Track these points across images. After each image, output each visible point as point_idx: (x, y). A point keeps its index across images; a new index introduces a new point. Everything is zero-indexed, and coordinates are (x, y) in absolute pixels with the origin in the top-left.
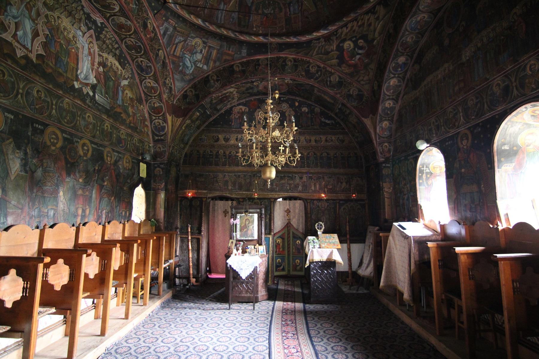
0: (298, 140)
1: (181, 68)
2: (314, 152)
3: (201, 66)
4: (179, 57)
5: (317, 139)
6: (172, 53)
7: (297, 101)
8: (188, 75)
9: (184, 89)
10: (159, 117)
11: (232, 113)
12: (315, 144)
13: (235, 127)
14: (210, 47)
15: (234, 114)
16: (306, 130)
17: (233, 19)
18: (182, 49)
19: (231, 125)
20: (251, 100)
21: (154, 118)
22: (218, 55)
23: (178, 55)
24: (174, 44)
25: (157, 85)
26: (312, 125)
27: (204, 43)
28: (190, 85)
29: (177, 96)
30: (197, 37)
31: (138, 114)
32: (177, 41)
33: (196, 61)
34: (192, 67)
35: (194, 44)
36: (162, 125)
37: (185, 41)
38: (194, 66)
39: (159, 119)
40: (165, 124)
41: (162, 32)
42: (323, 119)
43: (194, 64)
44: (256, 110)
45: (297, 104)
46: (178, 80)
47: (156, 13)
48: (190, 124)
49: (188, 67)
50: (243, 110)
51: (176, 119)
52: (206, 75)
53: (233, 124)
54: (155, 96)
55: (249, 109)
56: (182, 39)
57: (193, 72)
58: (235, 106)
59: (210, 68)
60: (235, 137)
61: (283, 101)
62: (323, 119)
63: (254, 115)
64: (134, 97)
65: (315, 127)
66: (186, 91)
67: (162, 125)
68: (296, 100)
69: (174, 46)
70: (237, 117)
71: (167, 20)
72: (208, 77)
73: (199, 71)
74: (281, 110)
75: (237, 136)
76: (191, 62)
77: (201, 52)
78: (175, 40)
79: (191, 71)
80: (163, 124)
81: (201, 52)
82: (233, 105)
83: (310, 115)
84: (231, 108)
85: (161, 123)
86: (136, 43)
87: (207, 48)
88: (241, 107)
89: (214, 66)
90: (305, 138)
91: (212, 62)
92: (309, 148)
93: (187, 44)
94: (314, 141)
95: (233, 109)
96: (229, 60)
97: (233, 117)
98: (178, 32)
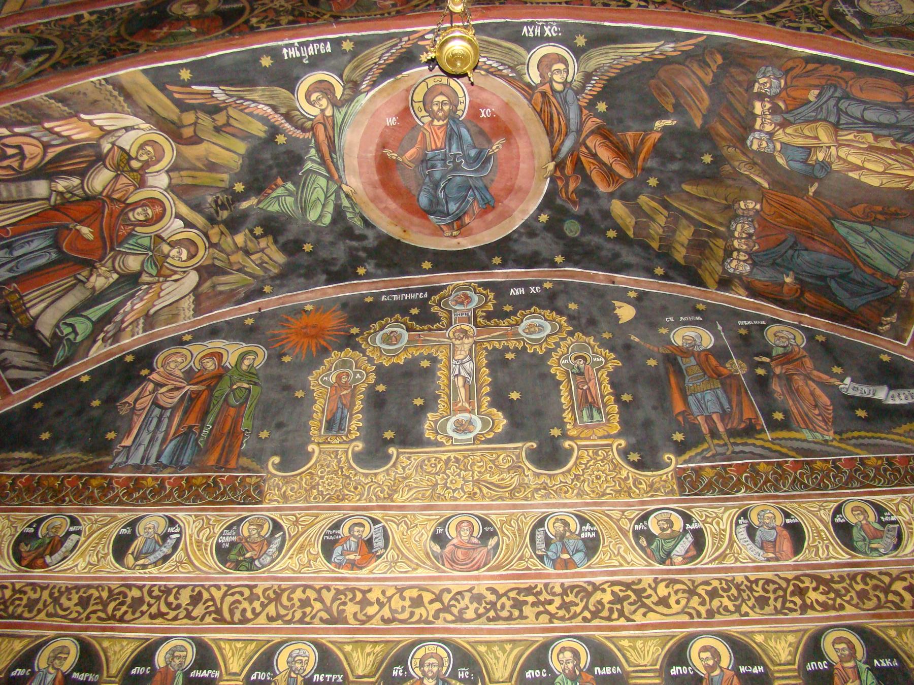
0: (677, 537)
2: (861, 632)
5: (849, 516)
7: (629, 301)
11: (145, 378)
12: (844, 556)
13: (136, 460)
15: (159, 385)
16: (736, 455)
19: (106, 447)
20: (299, 311)
26: (774, 426)
42: (848, 386)
44: (324, 352)
45: (626, 312)
50: (230, 360)
53: (128, 442)
55: (276, 357)
58: (179, 341)
60: (116, 529)
61: (528, 302)
62: (848, 386)
63: (305, 387)
65: (807, 435)
68: (622, 295)
70: (169, 399)
74: (512, 344)
75: (133, 524)
82: (164, 331)
83: (737, 366)
84: (145, 357)
88: (217, 344)
90: (744, 514)
92: (801, 592)
94: (828, 534)
95: (160, 358)
97: (146, 401)
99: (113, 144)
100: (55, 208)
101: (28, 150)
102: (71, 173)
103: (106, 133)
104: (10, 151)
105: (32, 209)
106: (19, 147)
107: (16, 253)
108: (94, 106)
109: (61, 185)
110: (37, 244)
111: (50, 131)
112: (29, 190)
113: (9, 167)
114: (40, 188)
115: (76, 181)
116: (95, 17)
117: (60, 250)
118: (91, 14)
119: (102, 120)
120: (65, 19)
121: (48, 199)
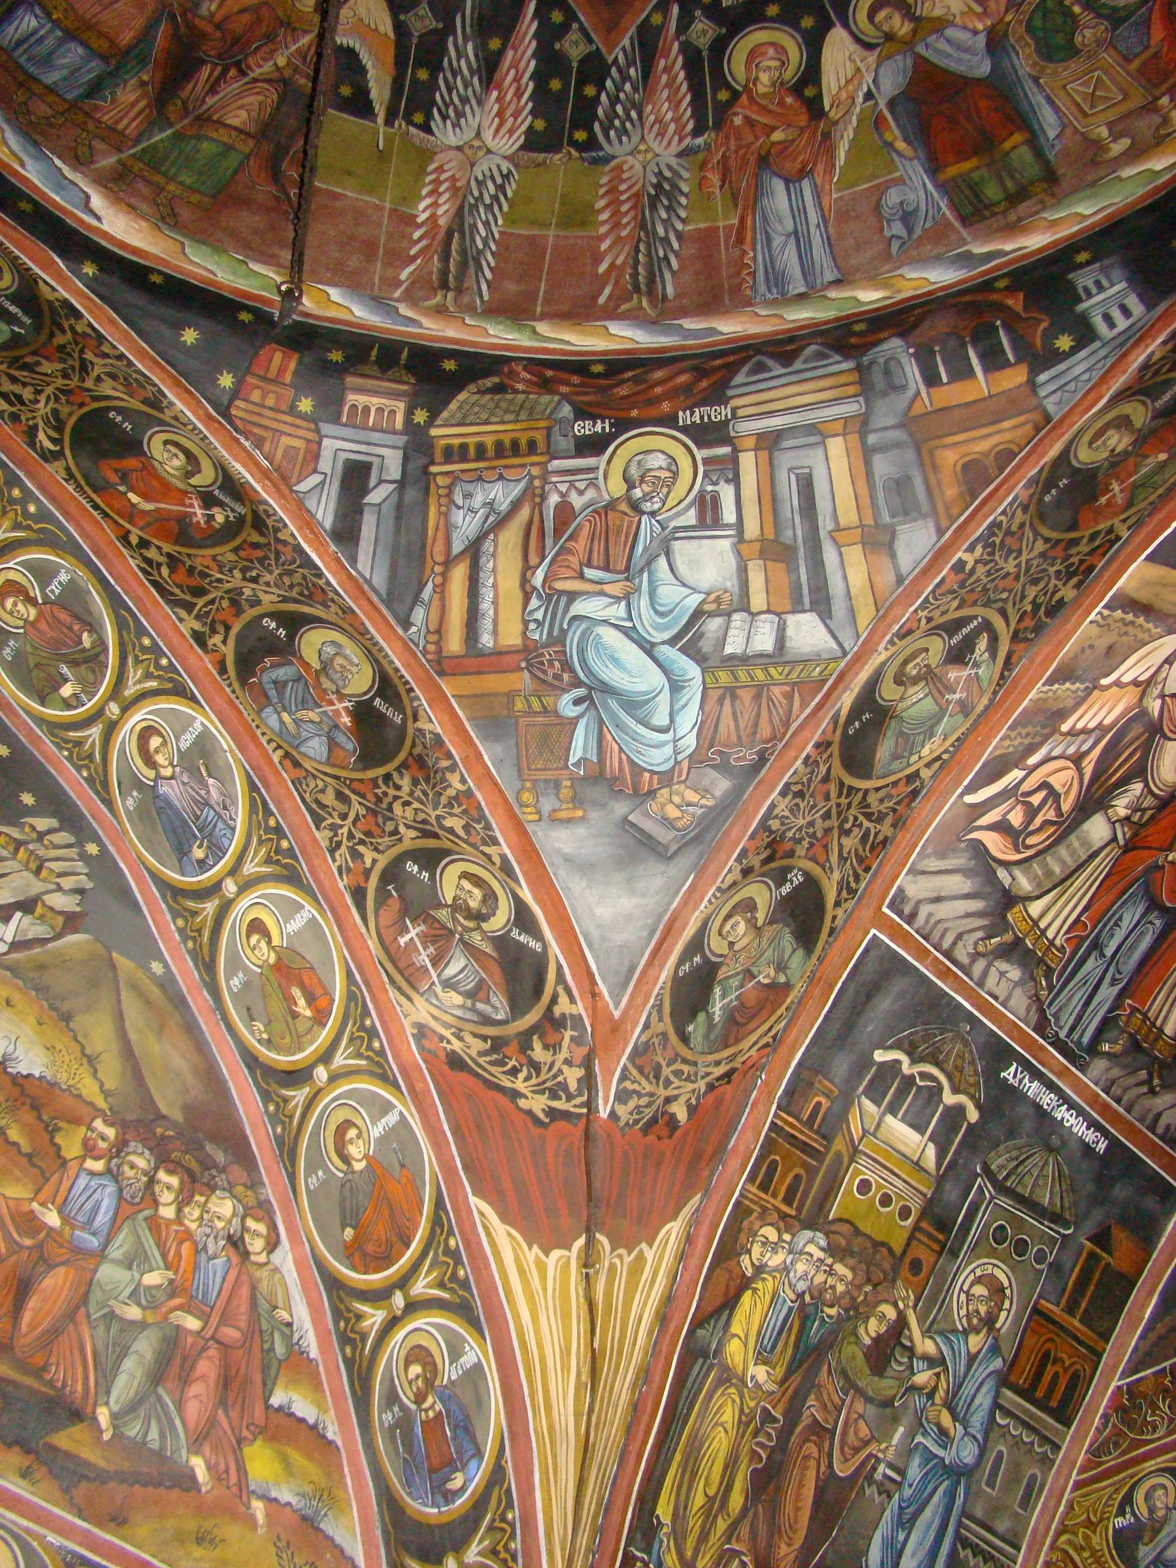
1: (580, 745)
3: (764, 641)
4: (529, 652)
6: (454, 644)
8: (667, 778)
9: (670, 931)
10: (403, 1283)
14: (770, 442)
17: (907, 218)
18: (527, 569)
21: (374, 1317)
22: (882, 466)
23: (511, 637)
24: (449, 562)
25: (309, 910)
27: (705, 435)
28: (729, 869)
29: (617, 1028)
30: (623, 425)
31: (135, 1260)
32: (466, 525)
33: (698, 614)
34: (676, 687)
35: (616, 487)
36: (450, 1373)
37: (534, 496)
38: (693, 671)
39: (413, 1307)
40: (474, 1352)
41: (325, 512)
43: (692, 650)
46: (583, 867)
47: (236, 393)
48: (856, 1311)
49: (635, 705)
51: (624, 1260)
52: (847, 700)
54: (326, 1057)
56: (502, 494)
57: (707, 730)
59: (865, 616)
64: (89, 1088)
66: (697, 944)
67: (450, 1373)
69: (459, 574)
71: (331, 408)
72: (868, 699)
73: (760, 691)
76: (648, 649)
77: (708, 508)
78: (449, 529)
79: (689, 719)
80: (455, 1354)
81: (708, 508)
85: (439, 1349)
86: (44, 574)
87: (747, 461)
89: (886, 578)
91: (855, 554)
93: (565, 512)
96: (1005, 457)
98: (449, 454)
99: (1162, 696)
100: (1129, 847)
101: (1056, 781)
102: (1125, 781)
103: (1141, 687)
104: (1036, 800)
105: (1101, 866)
106: (1045, 785)
107: (1109, 952)
108: (1113, 656)
109: (1121, 806)
110: (1129, 918)
111: (1072, 733)
112: (1085, 843)
113: (1047, 823)
114: (1097, 829)
115: (1137, 787)
116: (979, 550)
117: (1163, 910)
118: (971, 549)
119: (1132, 669)
120: (942, 581)
121: (1114, 839)
